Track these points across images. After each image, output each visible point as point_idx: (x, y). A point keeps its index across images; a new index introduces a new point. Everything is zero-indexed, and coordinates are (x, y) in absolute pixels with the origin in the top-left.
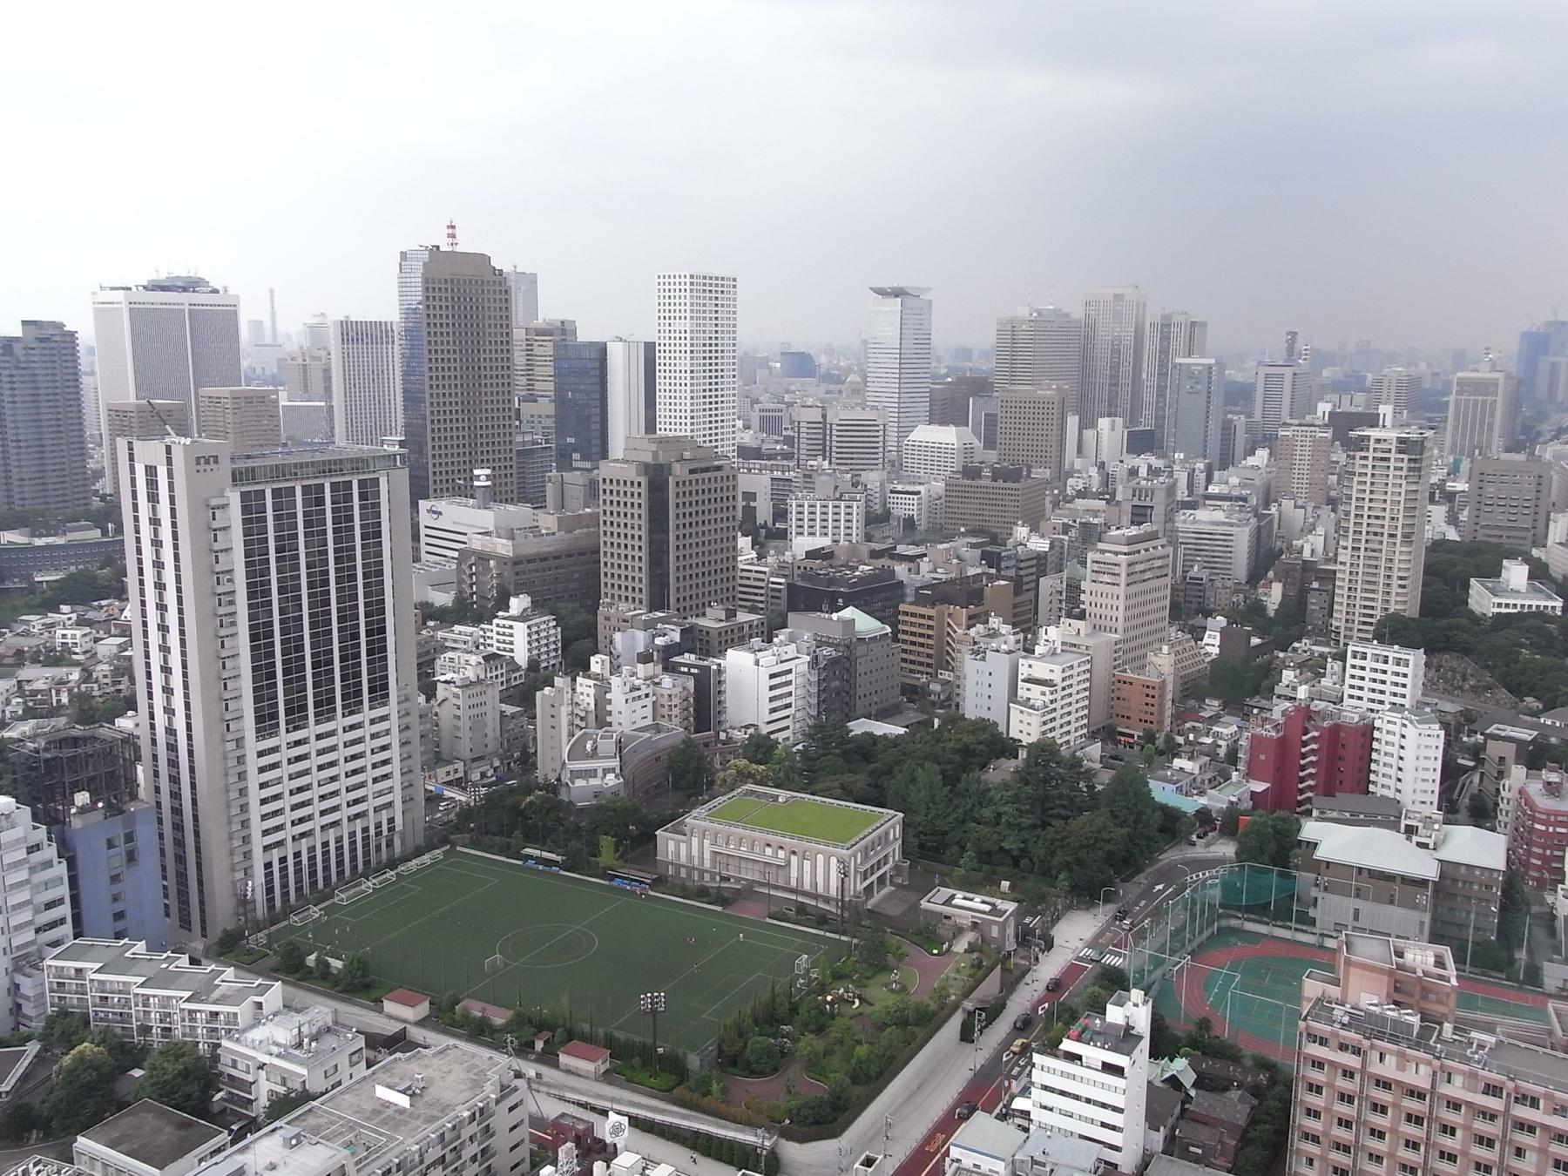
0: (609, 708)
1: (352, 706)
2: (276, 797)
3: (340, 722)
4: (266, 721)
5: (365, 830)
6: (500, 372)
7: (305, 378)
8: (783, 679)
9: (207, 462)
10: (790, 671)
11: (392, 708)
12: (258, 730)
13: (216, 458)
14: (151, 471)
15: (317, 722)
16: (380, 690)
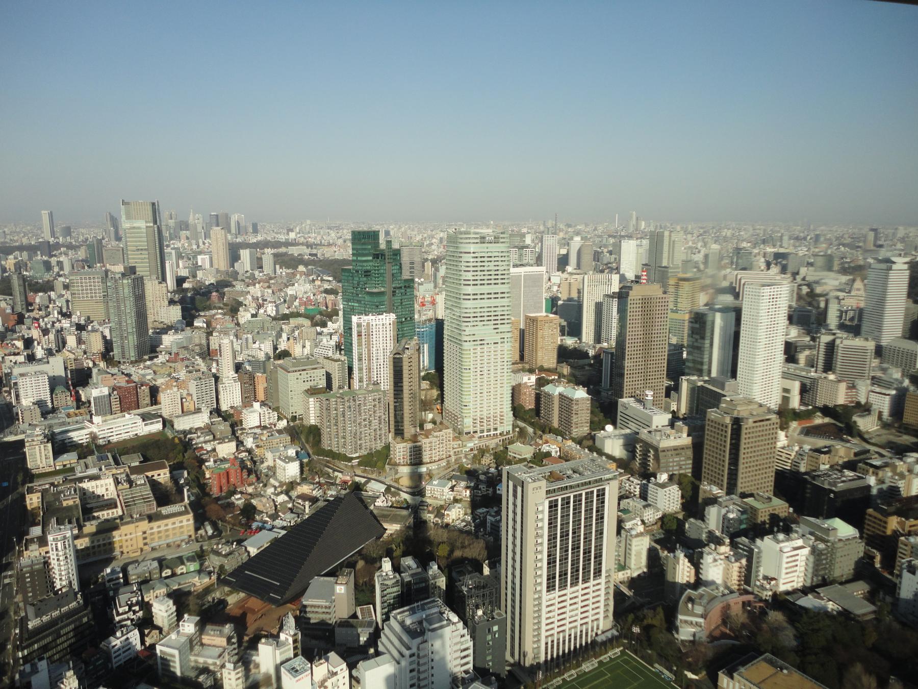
0: (701, 566)
1: (585, 581)
2: (552, 623)
3: (581, 585)
4: (550, 587)
5: (587, 630)
6: (662, 331)
7: (570, 291)
8: (794, 558)
9: (537, 489)
10: (798, 555)
11: (603, 580)
12: (547, 591)
13: (540, 488)
14: (515, 487)
15: (571, 587)
16: (598, 573)
